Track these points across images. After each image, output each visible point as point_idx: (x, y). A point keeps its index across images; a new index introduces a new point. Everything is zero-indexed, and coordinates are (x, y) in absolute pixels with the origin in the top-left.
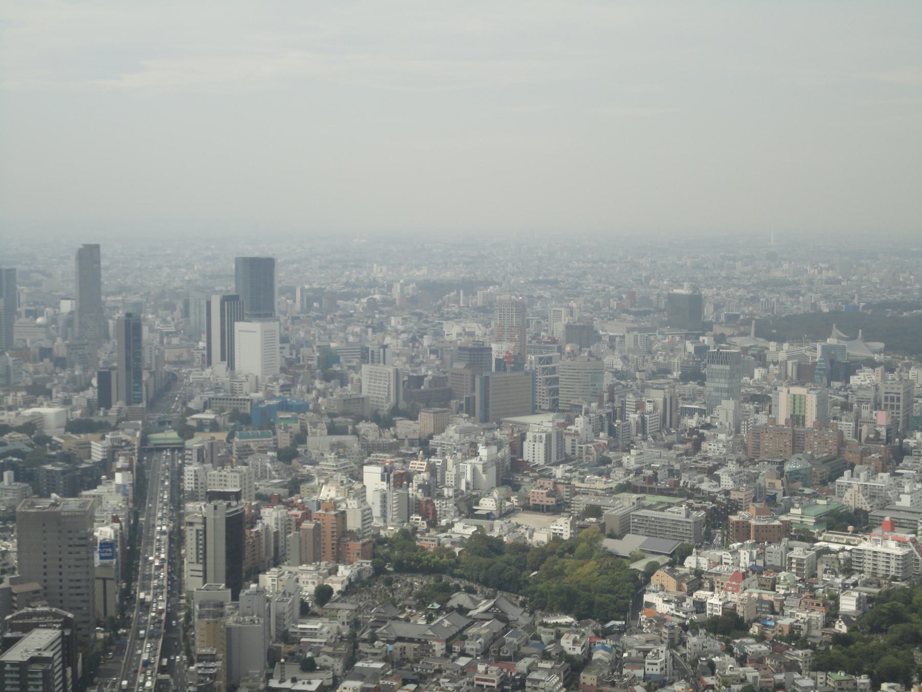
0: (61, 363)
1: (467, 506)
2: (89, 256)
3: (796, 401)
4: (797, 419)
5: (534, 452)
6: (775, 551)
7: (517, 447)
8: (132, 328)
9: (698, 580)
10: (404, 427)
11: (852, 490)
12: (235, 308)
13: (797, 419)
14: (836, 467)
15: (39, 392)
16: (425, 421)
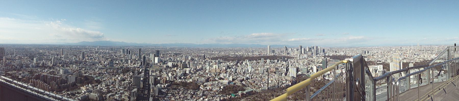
0: (137, 61)
1: (180, 78)
2: (140, 50)
3: (216, 66)
4: (216, 68)
5: (187, 72)
6: (214, 82)
7: (185, 72)
8: (144, 57)
9: (206, 86)
10: (173, 69)
11: (222, 76)
12: (155, 56)
13: (216, 68)
14: (220, 73)
15: (134, 64)
16: (175, 69)
